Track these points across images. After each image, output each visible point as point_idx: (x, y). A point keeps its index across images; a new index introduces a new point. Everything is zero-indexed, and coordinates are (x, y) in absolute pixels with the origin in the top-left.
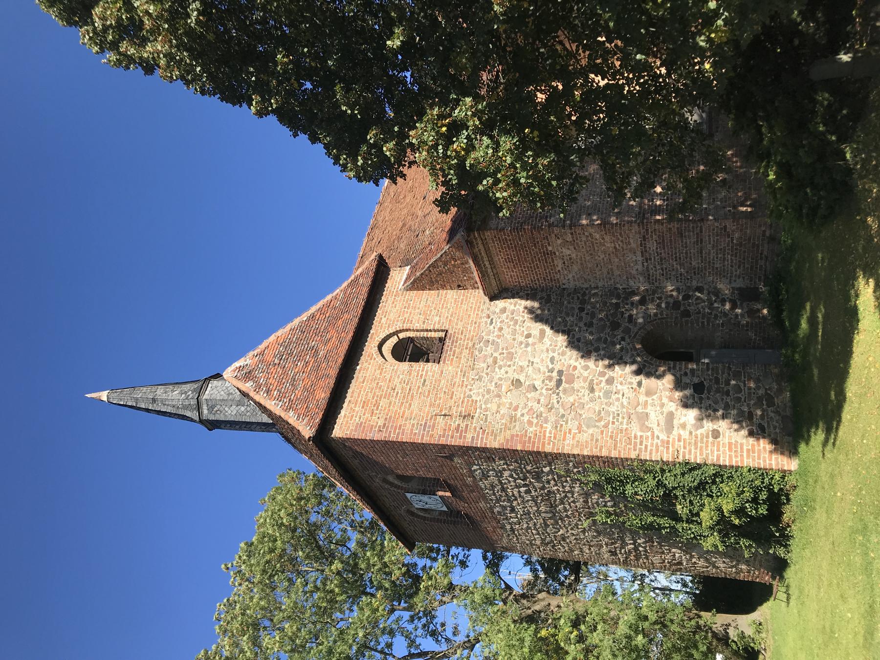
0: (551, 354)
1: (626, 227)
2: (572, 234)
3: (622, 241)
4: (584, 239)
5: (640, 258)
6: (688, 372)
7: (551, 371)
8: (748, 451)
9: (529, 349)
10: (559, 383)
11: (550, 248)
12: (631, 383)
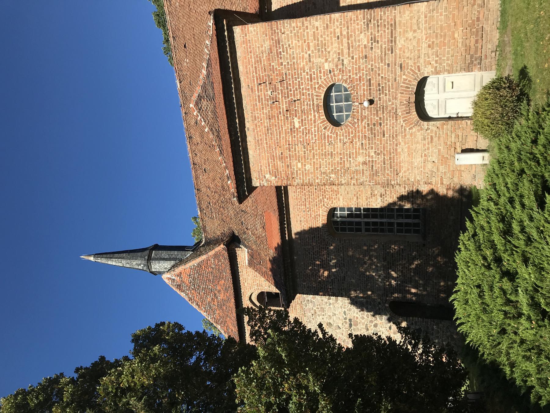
0: (344, 310)
6: (413, 322)
7: (345, 319)
9: (331, 306)
12: (386, 327)
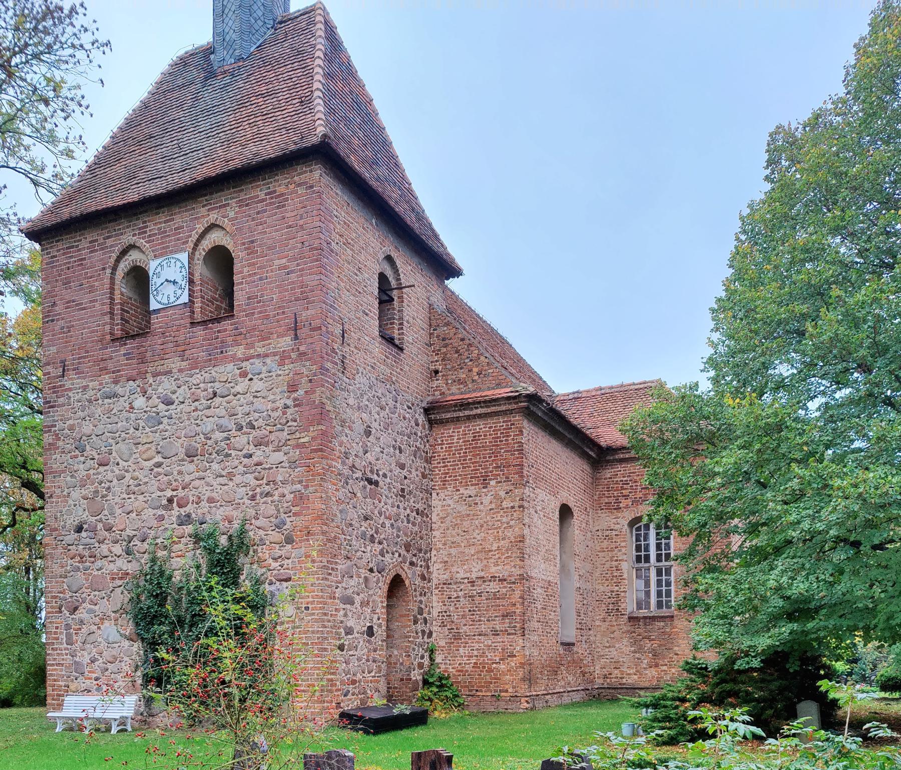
0: (389, 474)
1: (519, 563)
2: (513, 507)
3: (499, 558)
4: (504, 520)
5: (474, 576)
8: (332, 680)
10: (370, 482)
11: (493, 483)
